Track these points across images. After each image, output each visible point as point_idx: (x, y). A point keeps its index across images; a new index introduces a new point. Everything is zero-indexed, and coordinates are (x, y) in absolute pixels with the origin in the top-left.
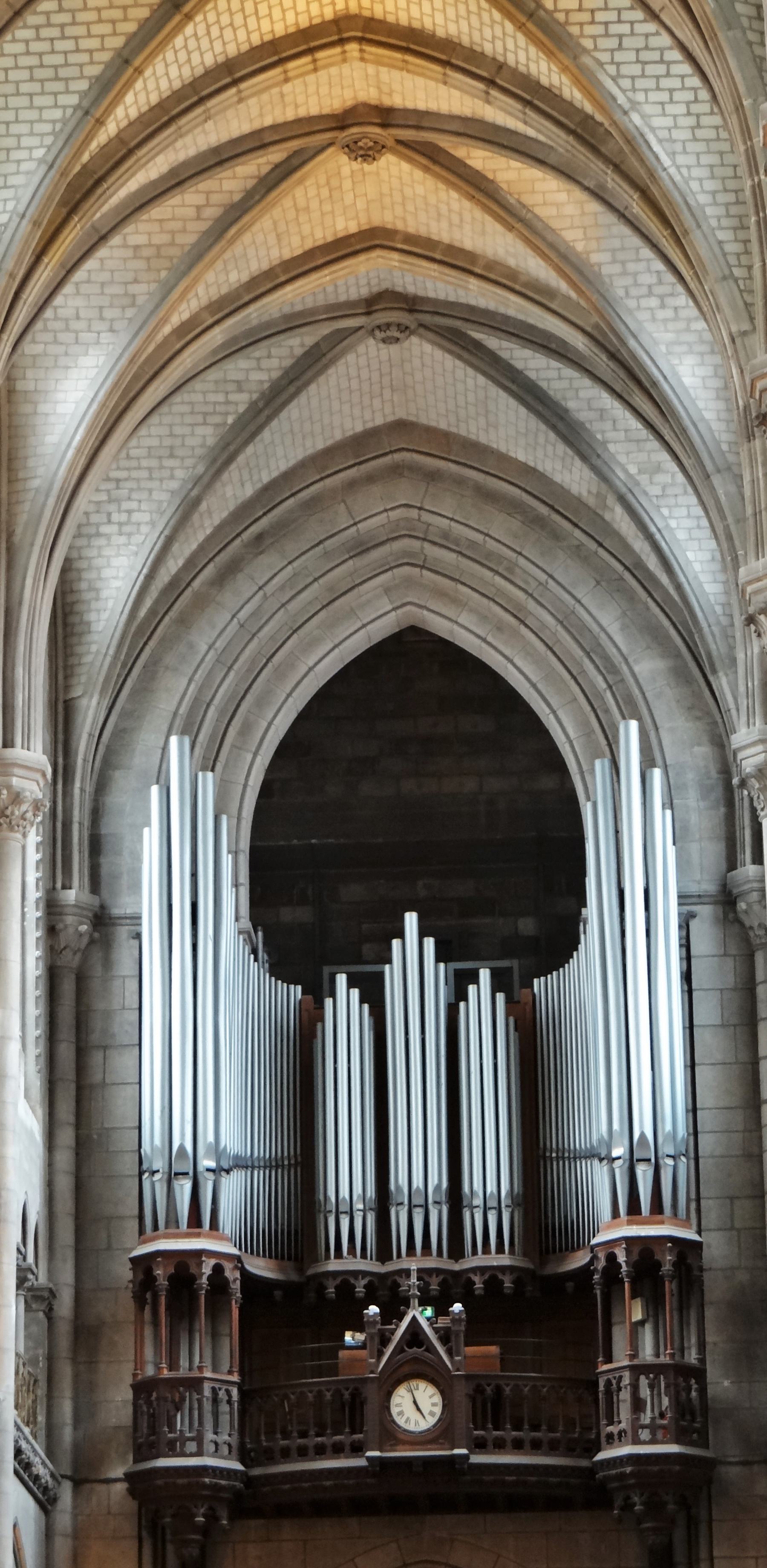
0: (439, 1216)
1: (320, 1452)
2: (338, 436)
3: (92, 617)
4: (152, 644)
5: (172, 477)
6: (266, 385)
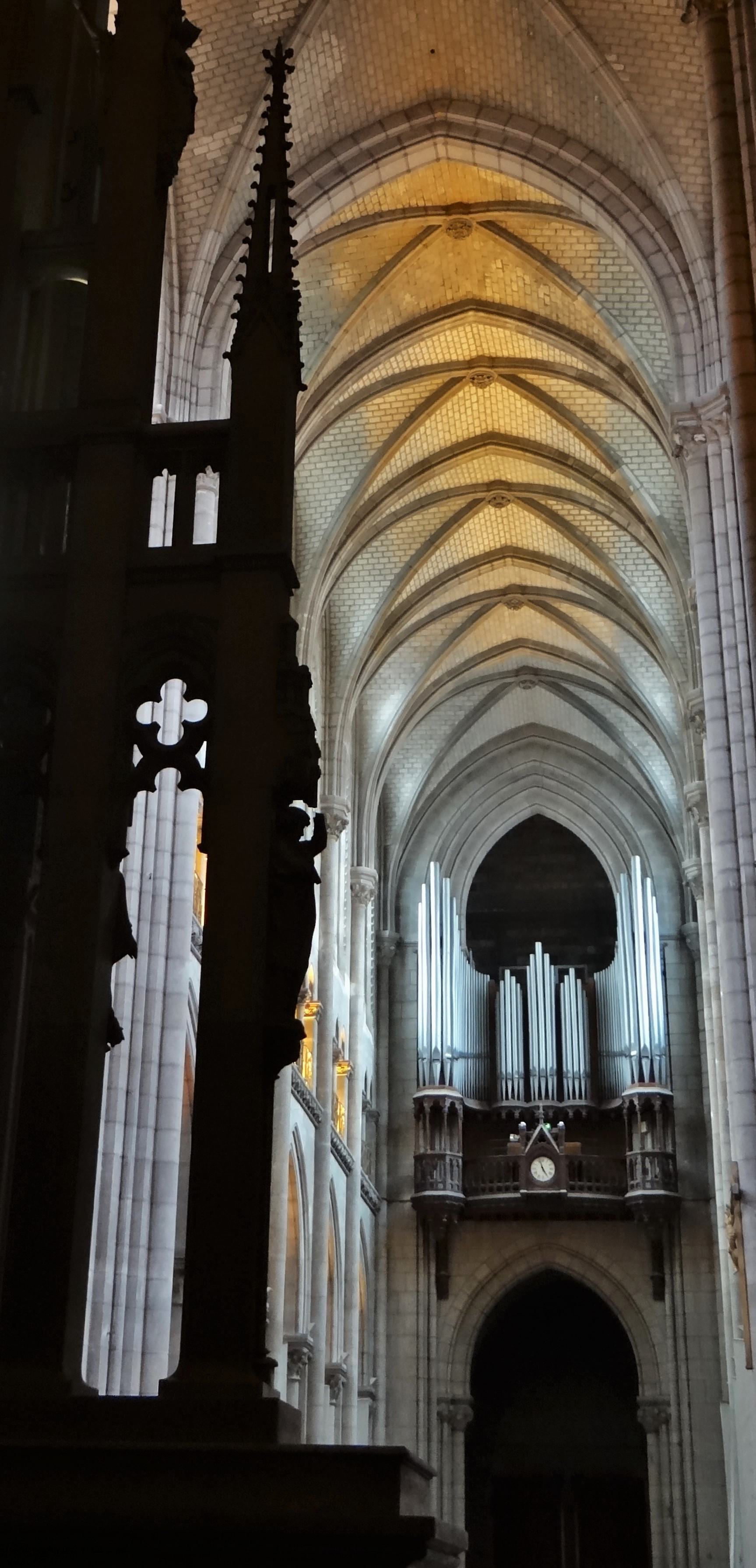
1: (499, 1190)
3: (396, 809)
5: (431, 748)
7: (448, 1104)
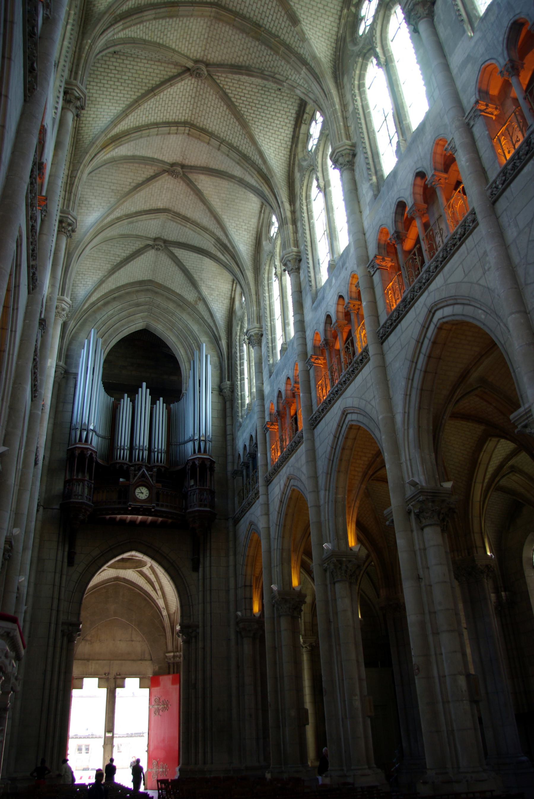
0: (146, 453)
2: (136, 280)
7: (90, 452)
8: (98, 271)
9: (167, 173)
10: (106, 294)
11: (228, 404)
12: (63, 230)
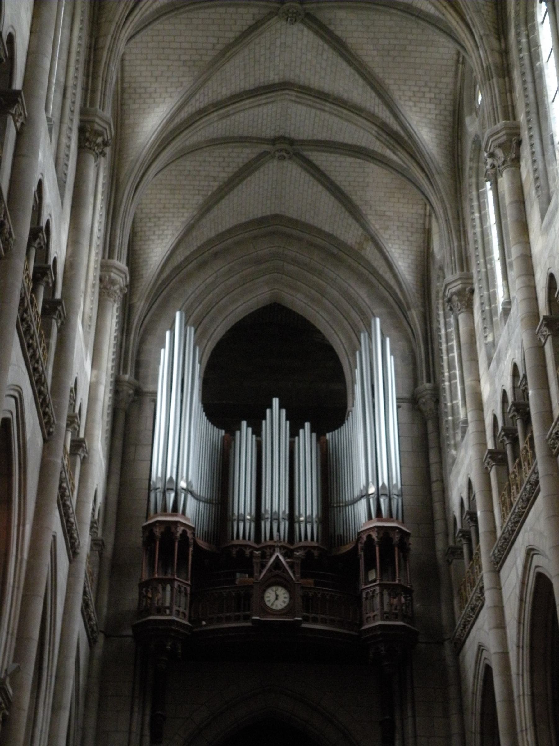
0: (284, 525)
1: (228, 619)
3: (144, 272)
4: (168, 289)
5: (183, 216)
6: (226, 179)
8: (181, 210)
9: (276, 17)
10: (199, 248)
11: (430, 426)
12: (87, 144)
